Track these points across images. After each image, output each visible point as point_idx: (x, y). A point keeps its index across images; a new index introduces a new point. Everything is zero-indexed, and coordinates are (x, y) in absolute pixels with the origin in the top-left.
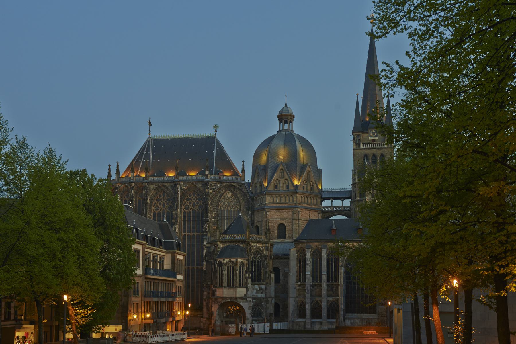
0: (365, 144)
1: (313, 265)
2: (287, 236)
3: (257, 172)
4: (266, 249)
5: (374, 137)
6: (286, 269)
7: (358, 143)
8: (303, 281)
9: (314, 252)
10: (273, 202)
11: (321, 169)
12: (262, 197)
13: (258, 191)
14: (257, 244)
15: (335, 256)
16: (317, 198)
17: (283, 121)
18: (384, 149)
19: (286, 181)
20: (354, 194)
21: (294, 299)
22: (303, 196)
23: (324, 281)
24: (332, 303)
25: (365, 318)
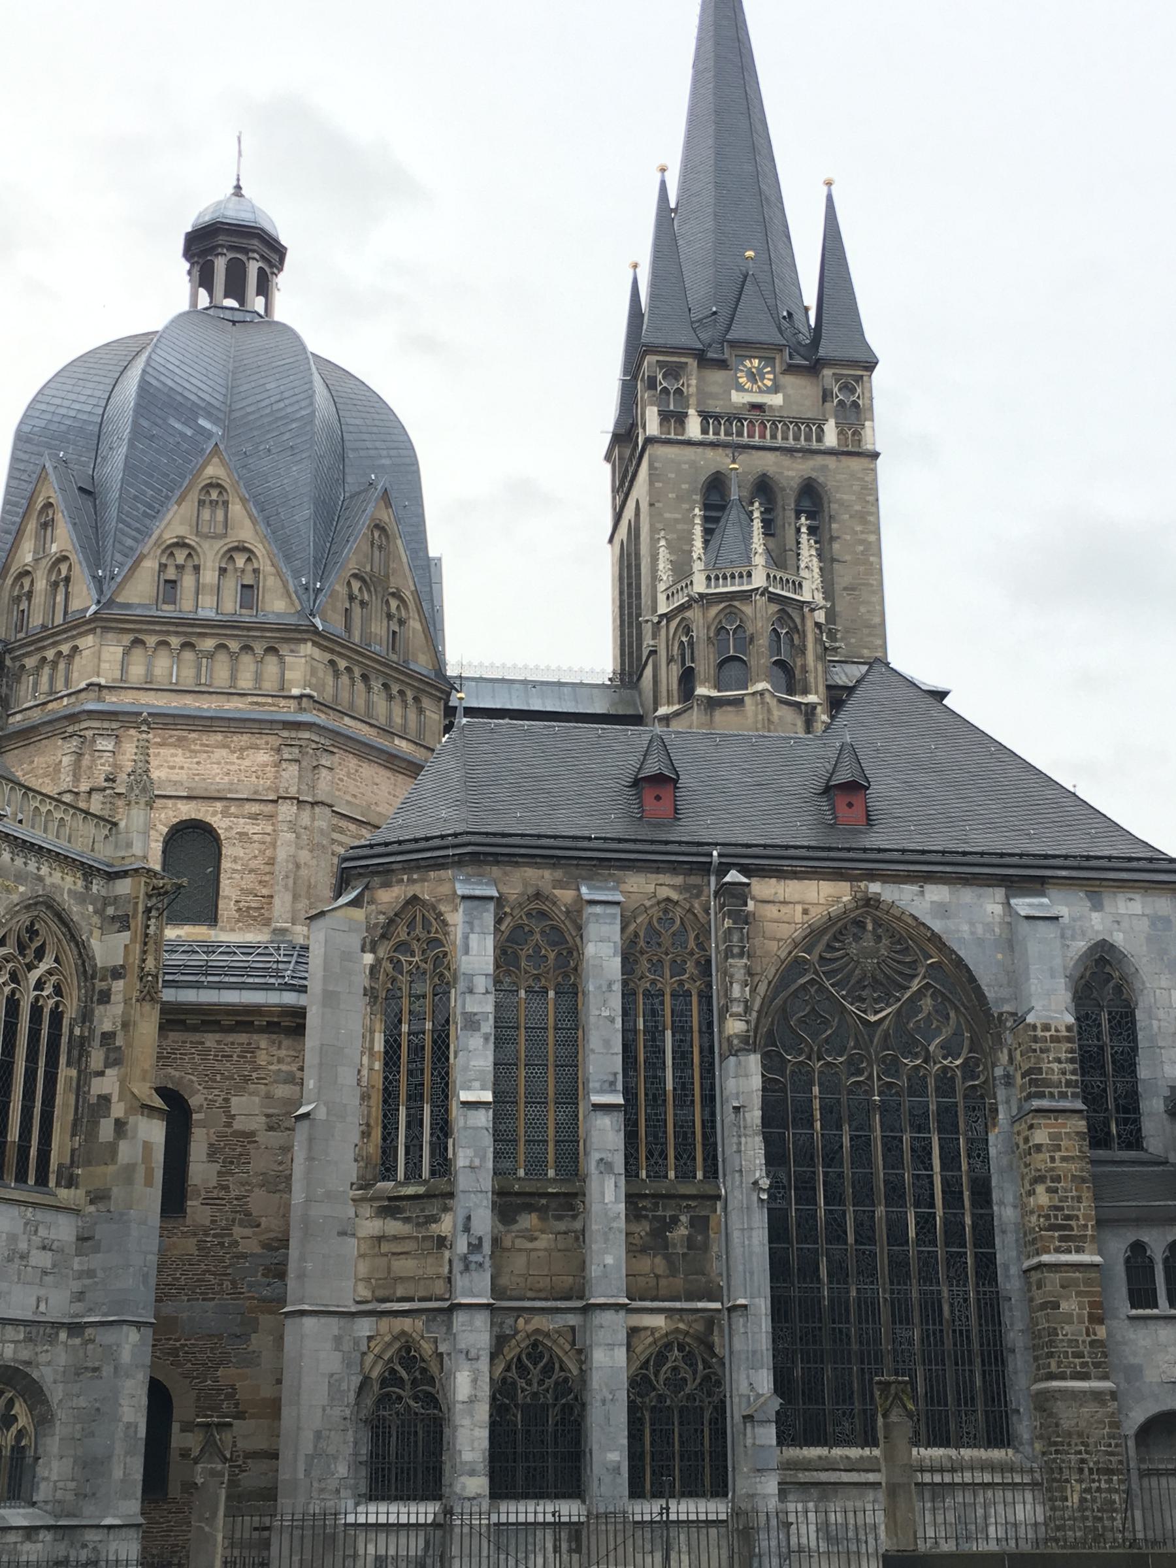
0: (717, 418)
1: (503, 1037)
2: (226, 909)
3: (39, 506)
4: (113, 918)
5: (761, 391)
6: (238, 1103)
7: (672, 408)
8: (413, 1172)
10: (146, 688)
11: (440, 559)
12: (65, 648)
13: (36, 620)
14: (44, 870)
15: (678, 968)
16: (426, 703)
17: (220, 264)
18: (820, 460)
19: (240, 561)
20: (676, 670)
21: (334, 1325)
22: (342, 664)
23: (606, 1166)
25: (939, 1491)
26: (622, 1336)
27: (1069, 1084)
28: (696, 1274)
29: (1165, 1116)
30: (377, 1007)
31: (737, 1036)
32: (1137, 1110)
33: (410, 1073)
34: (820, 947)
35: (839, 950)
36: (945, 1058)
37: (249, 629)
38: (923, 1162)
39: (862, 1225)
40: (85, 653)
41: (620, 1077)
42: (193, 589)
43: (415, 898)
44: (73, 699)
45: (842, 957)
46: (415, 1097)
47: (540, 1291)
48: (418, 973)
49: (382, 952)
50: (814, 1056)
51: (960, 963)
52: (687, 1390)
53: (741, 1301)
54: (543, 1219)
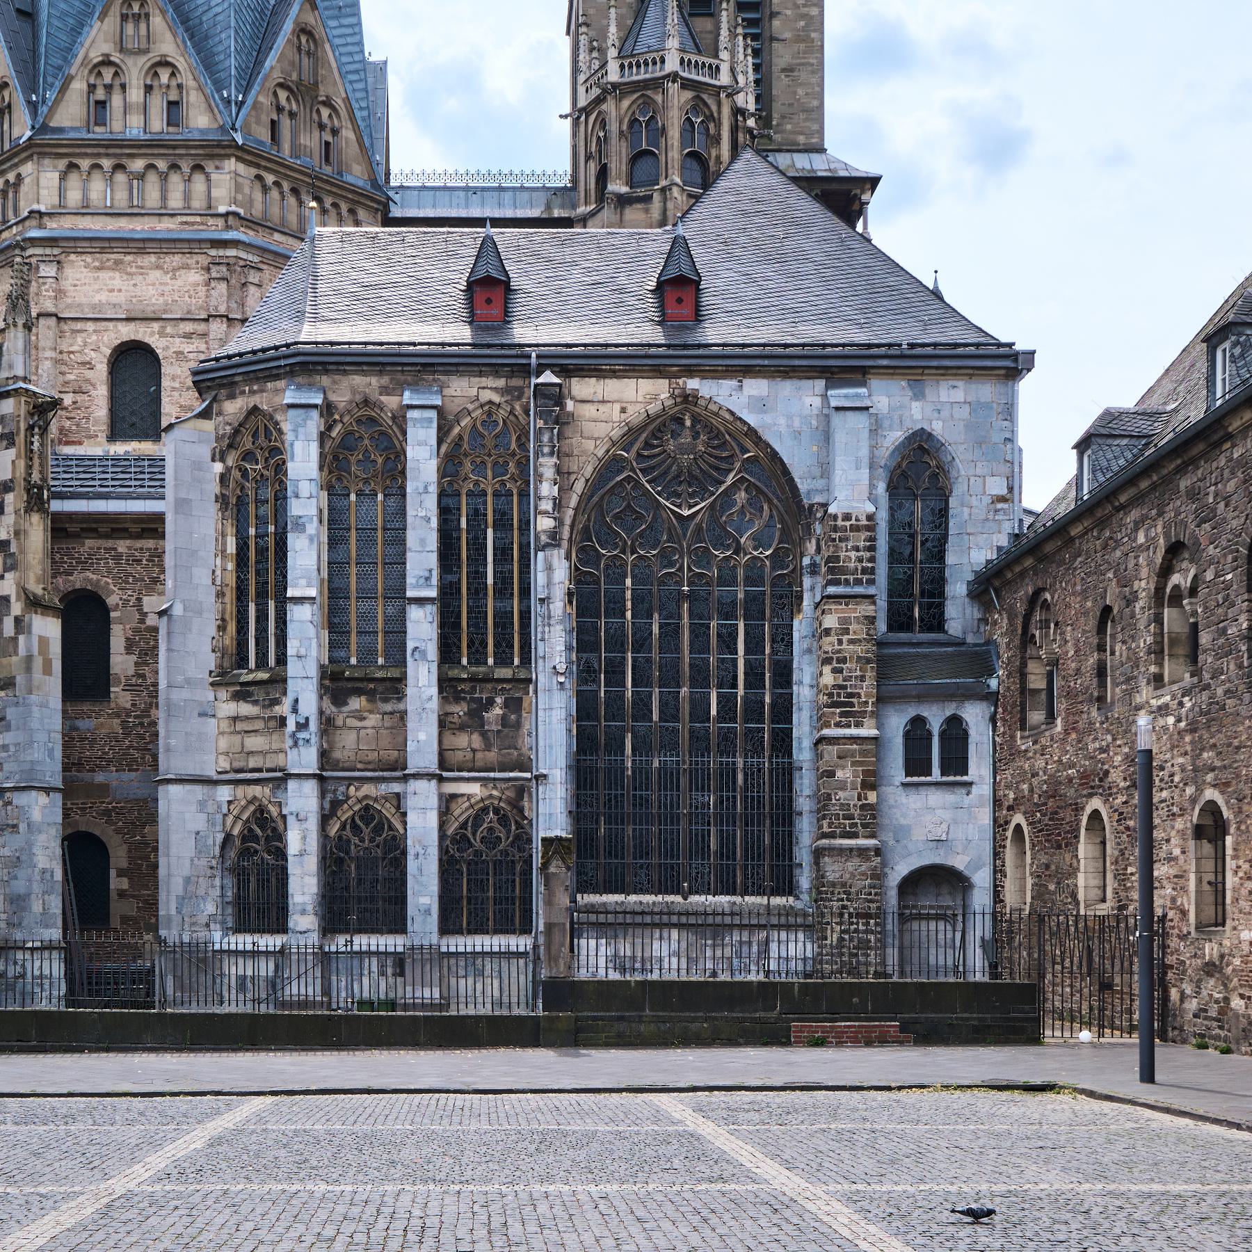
8: (262, 663)
9: (348, 443)
10: (85, 210)
12: (11, 177)
15: (500, 468)
20: (593, 167)
22: (270, 179)
24: (478, 818)
26: (434, 801)
27: (864, 571)
28: (509, 748)
29: (967, 600)
30: (228, 513)
31: (544, 531)
32: (942, 594)
33: (258, 573)
34: (635, 448)
35: (657, 447)
36: (755, 549)
37: (174, 147)
38: (728, 647)
39: (667, 704)
40: (27, 181)
41: (435, 574)
42: (122, 110)
43: (255, 410)
44: (20, 227)
45: (659, 455)
46: (262, 595)
47: (369, 763)
48: (261, 480)
49: (230, 462)
50: (628, 550)
51: (775, 456)
52: (501, 847)
53: (544, 772)
54: (371, 700)
